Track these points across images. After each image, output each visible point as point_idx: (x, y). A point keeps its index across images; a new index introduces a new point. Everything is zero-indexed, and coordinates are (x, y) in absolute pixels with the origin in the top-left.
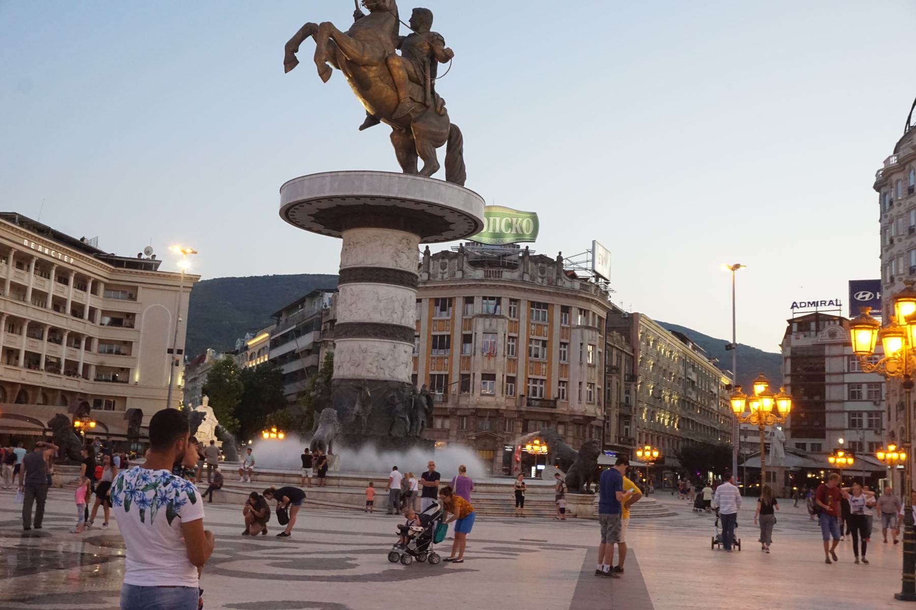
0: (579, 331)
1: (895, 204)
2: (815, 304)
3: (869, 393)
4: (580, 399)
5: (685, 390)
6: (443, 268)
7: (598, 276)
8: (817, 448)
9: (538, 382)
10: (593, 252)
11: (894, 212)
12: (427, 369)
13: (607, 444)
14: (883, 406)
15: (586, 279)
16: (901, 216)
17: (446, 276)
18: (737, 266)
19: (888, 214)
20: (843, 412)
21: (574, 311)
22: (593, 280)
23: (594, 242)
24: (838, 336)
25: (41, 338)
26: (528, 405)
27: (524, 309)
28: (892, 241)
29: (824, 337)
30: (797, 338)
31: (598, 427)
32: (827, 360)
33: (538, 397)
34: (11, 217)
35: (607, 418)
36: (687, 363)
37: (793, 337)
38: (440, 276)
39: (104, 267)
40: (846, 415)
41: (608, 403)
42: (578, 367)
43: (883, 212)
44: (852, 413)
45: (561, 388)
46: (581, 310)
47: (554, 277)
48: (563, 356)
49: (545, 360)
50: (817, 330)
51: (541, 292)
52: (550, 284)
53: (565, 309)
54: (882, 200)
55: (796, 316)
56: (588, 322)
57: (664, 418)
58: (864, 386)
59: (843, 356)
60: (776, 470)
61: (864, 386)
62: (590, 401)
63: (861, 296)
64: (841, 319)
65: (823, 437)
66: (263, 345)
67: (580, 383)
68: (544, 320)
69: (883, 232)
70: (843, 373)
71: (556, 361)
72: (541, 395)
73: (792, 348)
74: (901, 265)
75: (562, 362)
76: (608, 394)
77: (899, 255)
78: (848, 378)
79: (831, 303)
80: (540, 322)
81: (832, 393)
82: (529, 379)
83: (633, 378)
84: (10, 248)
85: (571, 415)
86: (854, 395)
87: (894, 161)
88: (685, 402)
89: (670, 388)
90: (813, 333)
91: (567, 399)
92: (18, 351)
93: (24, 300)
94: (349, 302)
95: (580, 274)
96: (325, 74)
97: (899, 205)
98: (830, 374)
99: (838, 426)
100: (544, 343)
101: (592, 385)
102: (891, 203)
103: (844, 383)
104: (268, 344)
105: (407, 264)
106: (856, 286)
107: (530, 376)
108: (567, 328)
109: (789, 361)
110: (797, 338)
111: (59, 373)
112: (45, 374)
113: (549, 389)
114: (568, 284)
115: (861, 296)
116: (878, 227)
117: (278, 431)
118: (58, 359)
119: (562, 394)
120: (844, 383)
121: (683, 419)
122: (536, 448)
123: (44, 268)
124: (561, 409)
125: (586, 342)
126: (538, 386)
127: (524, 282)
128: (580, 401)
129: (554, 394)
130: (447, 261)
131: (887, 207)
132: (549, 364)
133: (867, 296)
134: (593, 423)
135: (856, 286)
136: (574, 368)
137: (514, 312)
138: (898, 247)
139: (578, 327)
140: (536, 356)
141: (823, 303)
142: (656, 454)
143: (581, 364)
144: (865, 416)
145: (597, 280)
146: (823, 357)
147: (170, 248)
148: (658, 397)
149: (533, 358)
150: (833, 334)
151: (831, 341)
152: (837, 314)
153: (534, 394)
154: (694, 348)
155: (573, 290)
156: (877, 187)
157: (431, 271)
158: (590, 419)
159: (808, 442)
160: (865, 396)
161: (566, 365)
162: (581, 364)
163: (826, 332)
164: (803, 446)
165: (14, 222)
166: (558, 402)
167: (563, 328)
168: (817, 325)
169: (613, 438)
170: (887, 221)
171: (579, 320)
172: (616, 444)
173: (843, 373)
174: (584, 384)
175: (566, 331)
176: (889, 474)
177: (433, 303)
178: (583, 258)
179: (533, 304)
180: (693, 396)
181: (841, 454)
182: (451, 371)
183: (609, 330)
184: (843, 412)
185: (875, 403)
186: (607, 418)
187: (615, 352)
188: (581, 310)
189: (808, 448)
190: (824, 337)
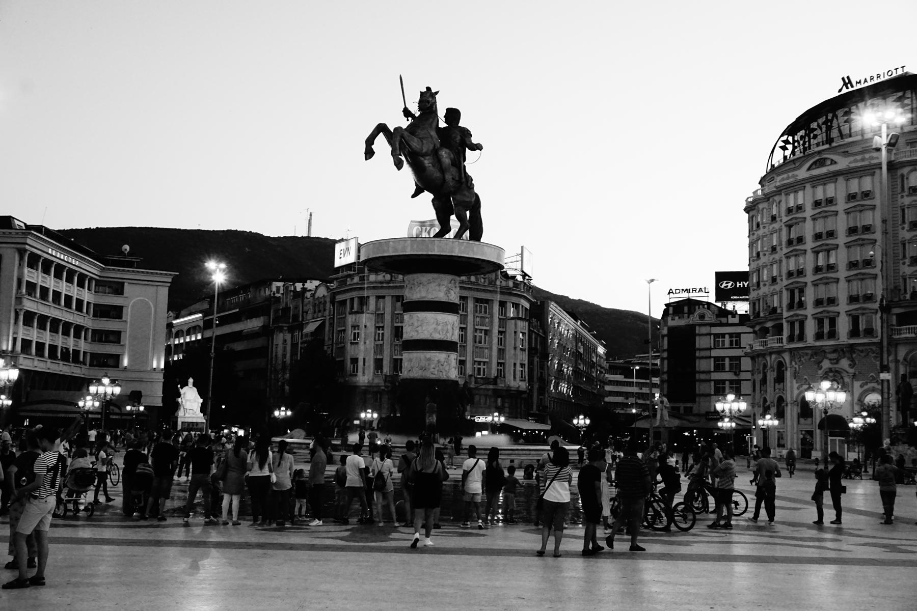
0: (513, 321)
1: (761, 226)
2: (688, 291)
3: (731, 365)
4: (514, 377)
5: (576, 361)
7: (525, 275)
8: (689, 411)
10: (522, 254)
11: (761, 232)
12: (391, 356)
14: (743, 376)
15: (514, 277)
16: (766, 236)
18: (652, 281)
19: (756, 233)
20: (710, 381)
21: (509, 305)
22: (520, 278)
23: (522, 247)
24: (706, 318)
25: (32, 327)
26: (476, 382)
27: (470, 305)
28: (758, 254)
29: (695, 319)
30: (673, 319)
32: (697, 338)
34: (39, 229)
35: (531, 390)
36: (578, 338)
37: (669, 319)
39: (95, 265)
40: (712, 383)
42: (513, 351)
43: (751, 232)
44: (717, 382)
46: (513, 304)
48: (500, 342)
49: (487, 345)
50: (691, 312)
51: (484, 291)
52: (490, 283)
53: (502, 304)
54: (751, 220)
55: (672, 301)
56: (518, 313)
57: (564, 388)
58: (727, 360)
59: (710, 334)
60: (662, 430)
61: (727, 361)
63: (724, 285)
64: (709, 304)
65: (694, 401)
66: (193, 325)
67: (515, 364)
68: (485, 312)
69: (751, 245)
70: (710, 349)
74: (765, 272)
76: (531, 370)
77: (764, 266)
78: (715, 353)
79: (700, 290)
80: (483, 314)
81: (702, 365)
83: (545, 356)
84: (40, 256)
85: (507, 390)
86: (719, 367)
87: (760, 192)
88: (576, 372)
89: (569, 360)
90: (686, 315)
91: (504, 377)
92: (44, 344)
93: (59, 305)
94: (416, 324)
95: (510, 273)
96: (399, 165)
97: (764, 227)
98: (700, 350)
99: (707, 392)
100: (486, 332)
101: (522, 365)
102: (758, 225)
103: (710, 357)
104: (201, 324)
105: (454, 297)
106: (720, 277)
109: (666, 339)
110: (673, 319)
111: (30, 354)
112: (61, 363)
113: (490, 369)
114: (504, 284)
115: (724, 285)
116: (746, 241)
117: (286, 409)
118: (67, 349)
119: (501, 374)
120: (710, 357)
121: (576, 389)
122: (496, 419)
123: (59, 271)
124: (501, 385)
125: (519, 330)
126: (482, 367)
127: (472, 283)
128: (516, 381)
129: (494, 373)
131: (755, 228)
132: (490, 349)
133: (729, 285)
134: (524, 396)
135: (720, 277)
136: (510, 352)
137: (465, 309)
138: (763, 260)
139: (512, 318)
140: (480, 342)
141: (694, 290)
142: (575, 422)
143: (515, 348)
144: (727, 383)
145: (524, 278)
146: (694, 335)
147: (206, 264)
148: (560, 370)
150: (702, 317)
152: (705, 299)
153: (479, 374)
154: (581, 324)
155: (507, 288)
156: (747, 210)
158: (519, 392)
159: (682, 406)
160: (727, 369)
162: (515, 348)
163: (696, 314)
164: (679, 408)
165: (41, 233)
166: (498, 381)
169: (535, 407)
170: (755, 237)
171: (511, 312)
173: (710, 349)
174: (518, 365)
175: (503, 321)
176: (754, 432)
177: (394, 299)
178: (514, 259)
179: (477, 300)
180: (581, 367)
181: (727, 420)
183: (531, 317)
184: (710, 381)
185: (736, 374)
186: (531, 390)
188: (513, 304)
189: (682, 411)
190: (695, 319)
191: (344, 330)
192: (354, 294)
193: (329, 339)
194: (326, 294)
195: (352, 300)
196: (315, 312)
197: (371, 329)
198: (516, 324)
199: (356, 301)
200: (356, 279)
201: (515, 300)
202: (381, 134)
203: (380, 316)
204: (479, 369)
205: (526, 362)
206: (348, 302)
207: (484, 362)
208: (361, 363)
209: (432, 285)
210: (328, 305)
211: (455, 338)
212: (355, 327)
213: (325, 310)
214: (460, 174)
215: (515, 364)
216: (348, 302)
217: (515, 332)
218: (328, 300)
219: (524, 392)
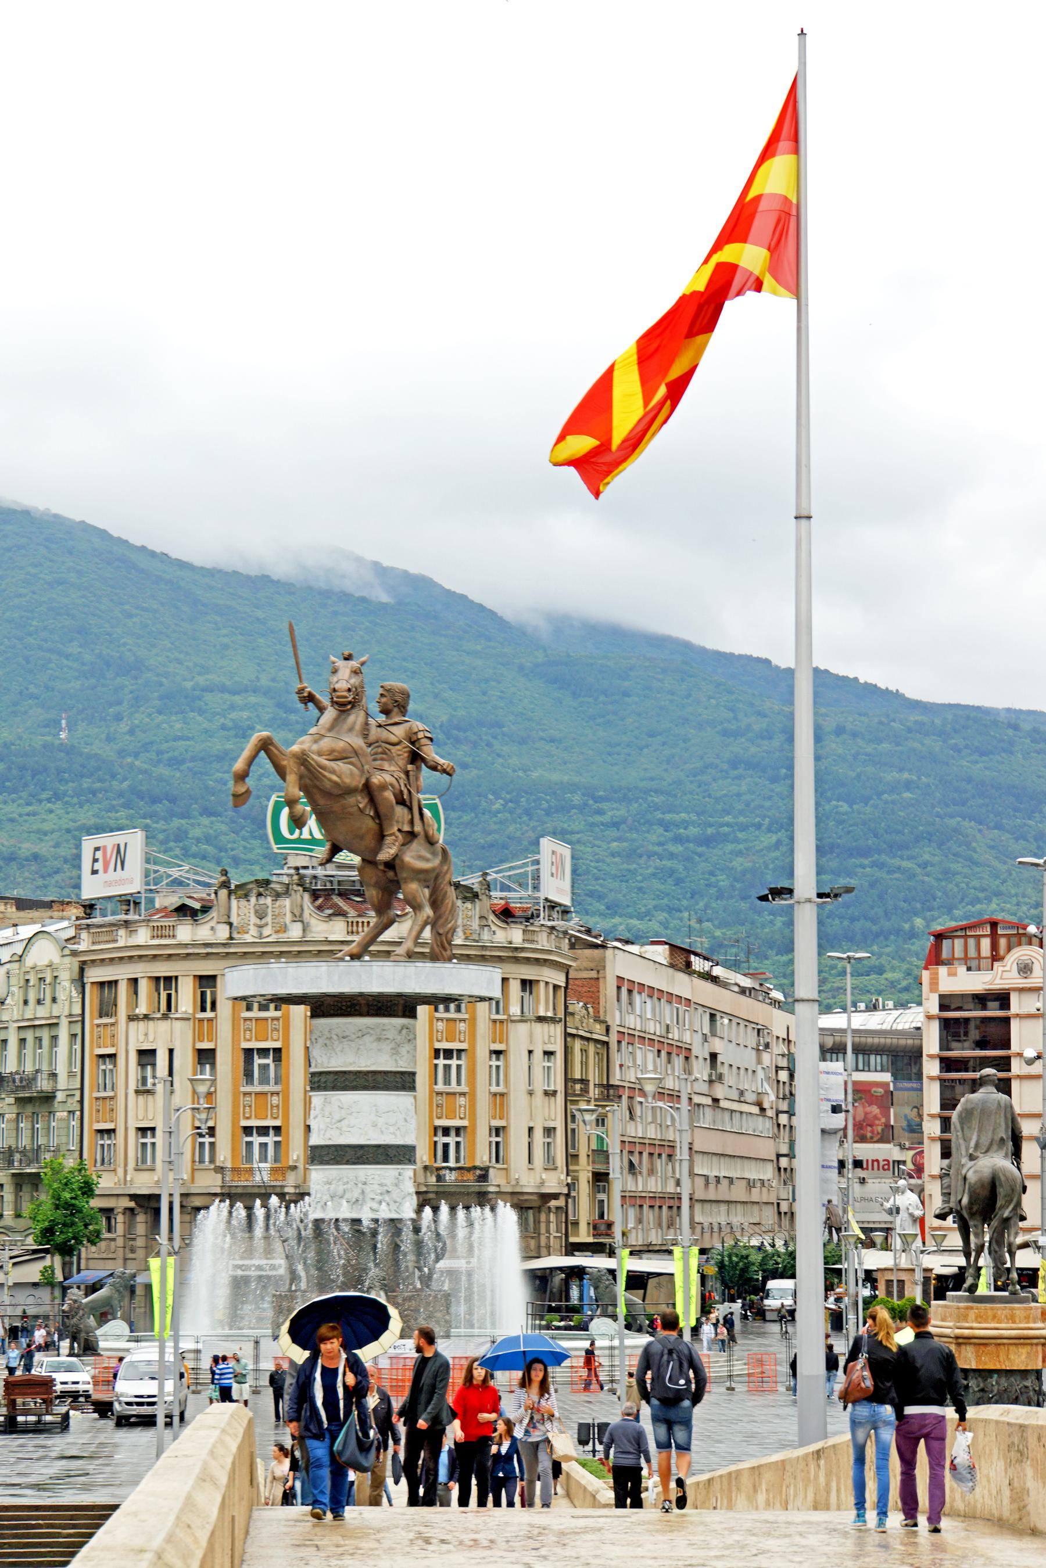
0: (523, 1028)
6: (261, 915)
9: (453, 1133)
13: (572, 1240)
17: (267, 931)
31: (558, 1208)
33: (452, 1164)
38: (253, 931)
41: (572, 1158)
45: (494, 1139)
47: (475, 924)
49: (463, 1088)
50: (996, 957)
62: (550, 1165)
67: (531, 1129)
71: (484, 1089)
72: (458, 1160)
73: (942, 997)
75: (494, 1089)
82: (436, 1128)
101: (549, 1131)
107: (439, 1123)
108: (502, 1022)
126: (451, 1140)
130: (269, 900)
134: (553, 1203)
136: (518, 1100)
140: (447, 1081)
149: (440, 1087)
150: (1025, 969)
151: (1022, 983)
157: (234, 919)
161: (502, 1095)
162: (531, 1093)
167: (495, 1021)
168: (994, 946)
169: (583, 1227)
172: (591, 1240)
174: (538, 1134)
182: (286, 1117)
187: (578, 1045)
191: (112, 1056)
192: (141, 970)
193: (71, 1075)
194: (56, 959)
195: (135, 981)
196: (26, 1002)
197: (185, 1060)
198: (531, 1035)
199: (144, 986)
200: (143, 936)
201: (529, 972)
202: (262, 754)
203: (204, 1027)
204: (446, 1146)
205: (559, 1124)
206: (123, 989)
207: (458, 1130)
208: (160, 1139)
209: (367, 1038)
210: (66, 984)
211: (409, 1141)
212: (146, 1056)
213: (54, 1000)
214: (412, 822)
215: (531, 1129)
216: (123, 989)
217: (530, 1052)
218: (65, 977)
219: (555, 1196)
